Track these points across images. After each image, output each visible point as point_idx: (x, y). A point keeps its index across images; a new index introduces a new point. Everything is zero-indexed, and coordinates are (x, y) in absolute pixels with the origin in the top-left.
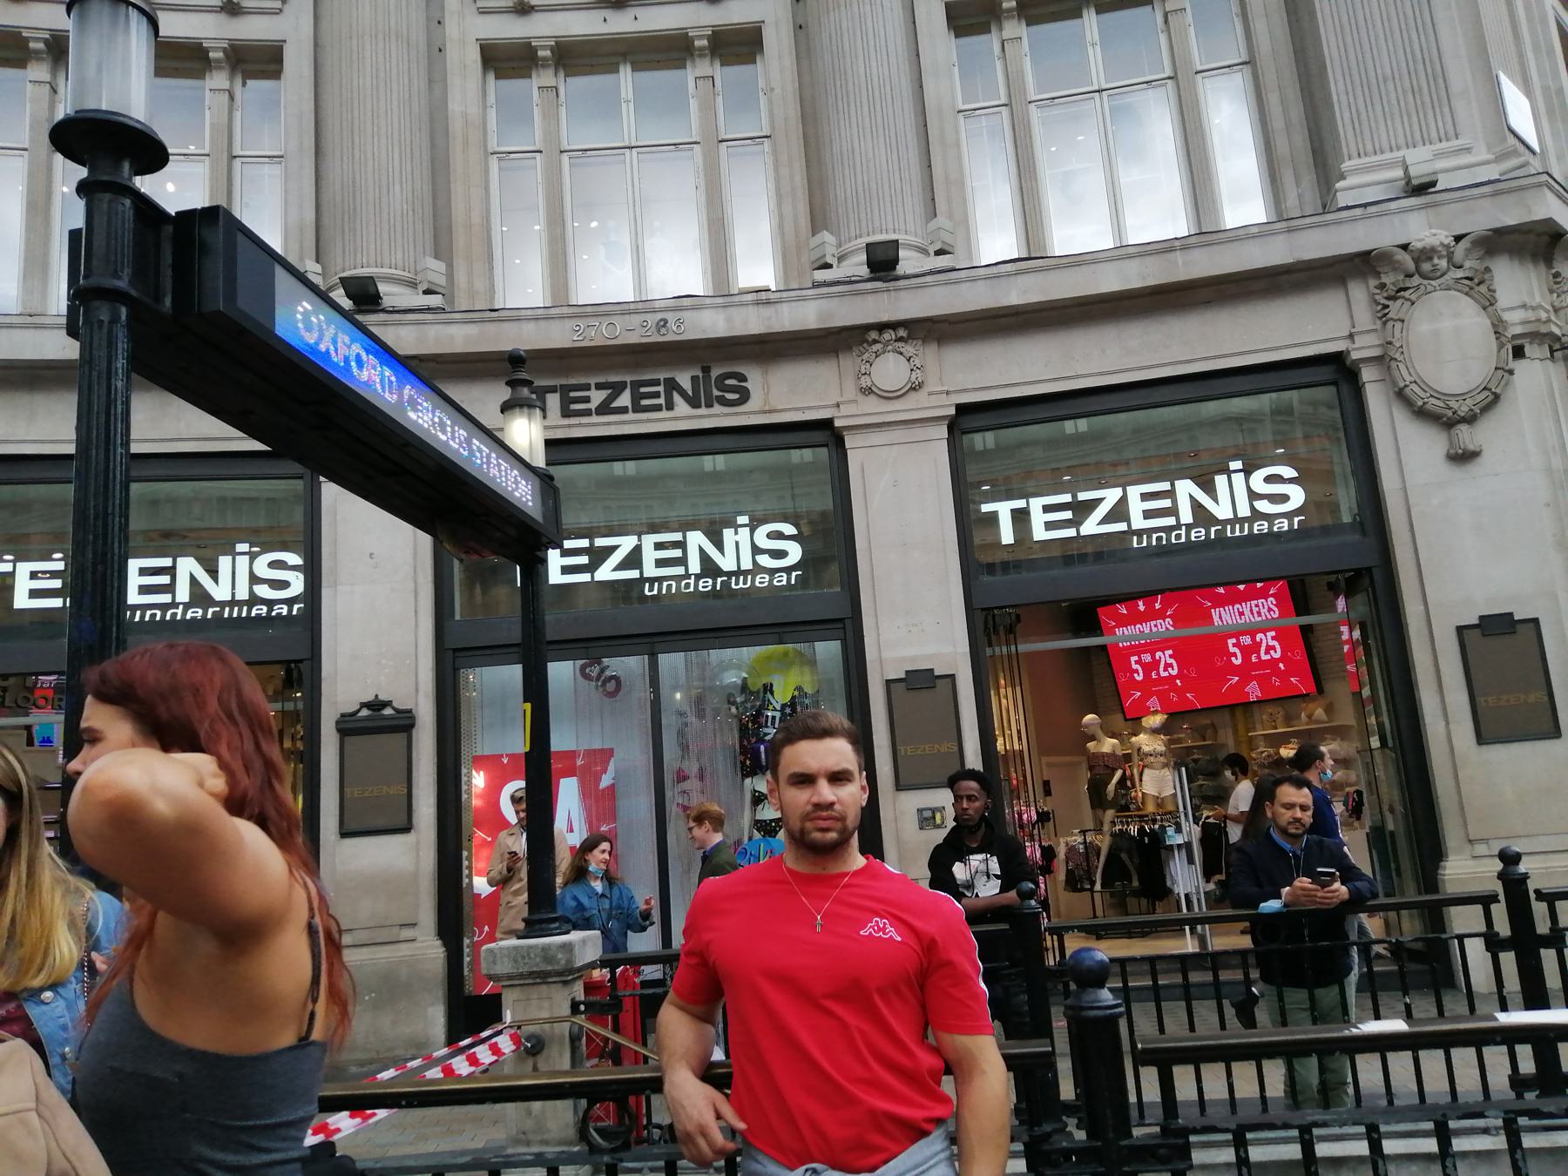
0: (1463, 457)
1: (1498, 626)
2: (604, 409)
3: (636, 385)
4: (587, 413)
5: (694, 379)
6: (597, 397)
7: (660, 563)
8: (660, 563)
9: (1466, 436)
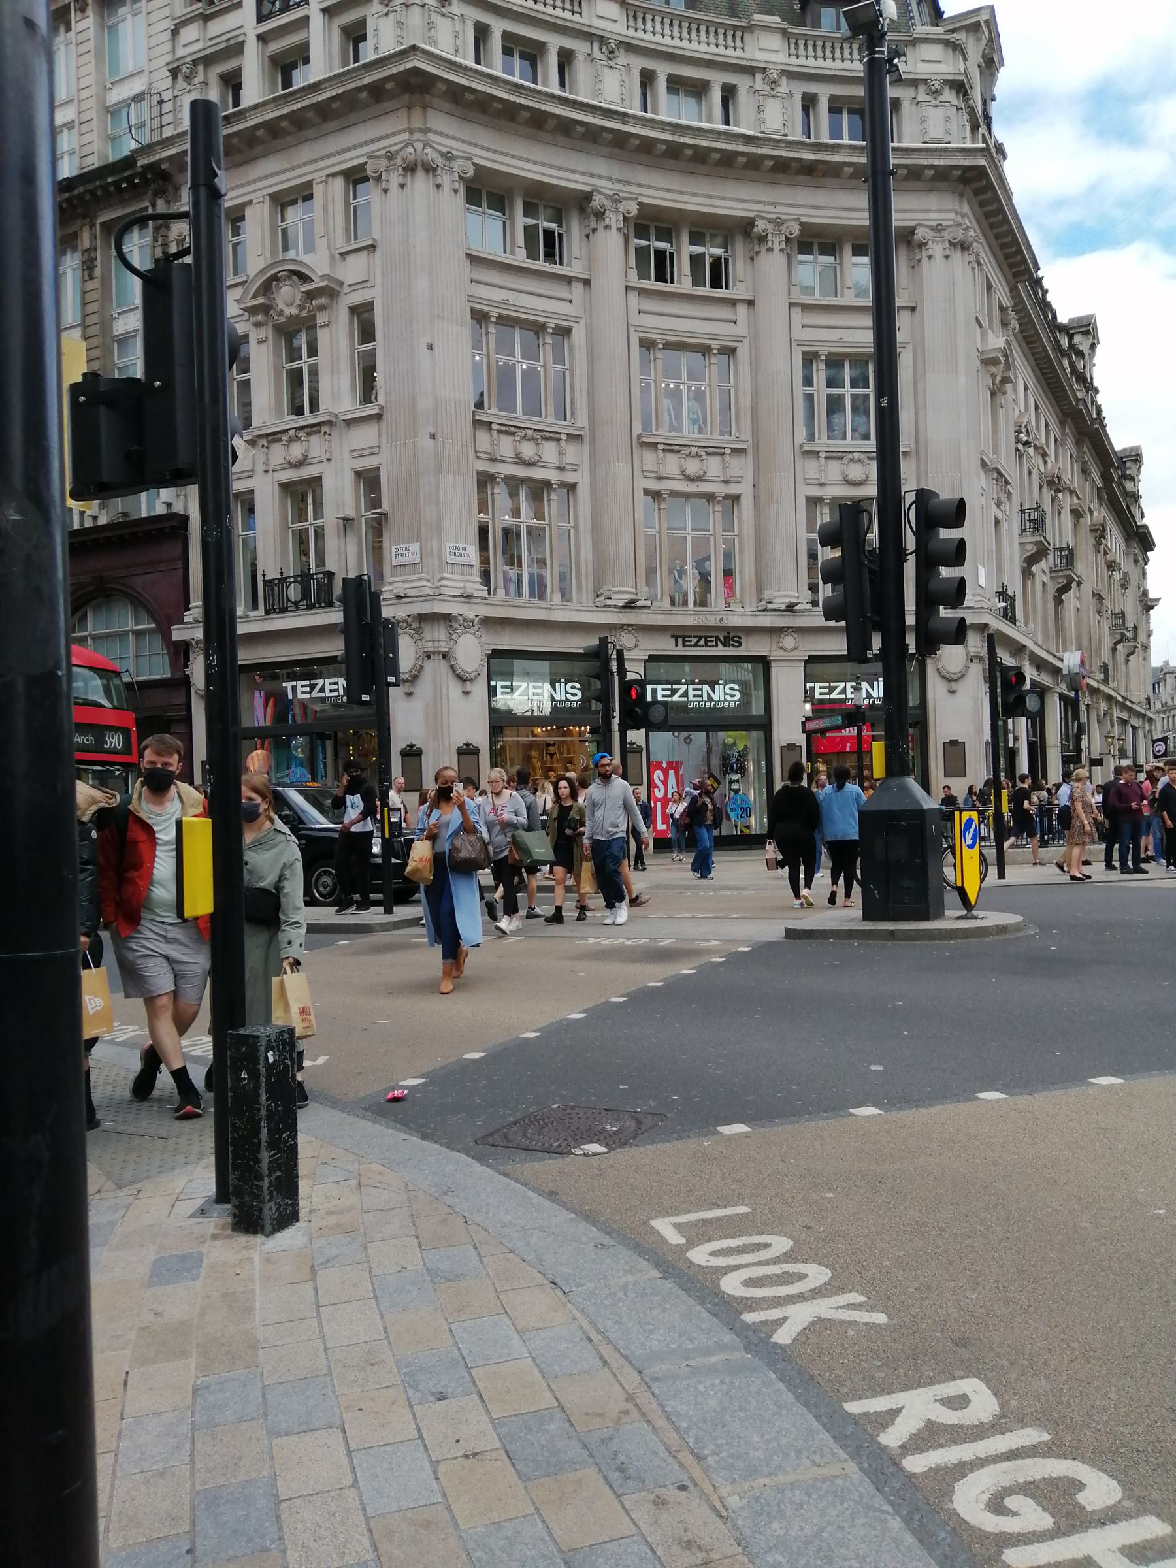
0: (952, 692)
1: (954, 743)
2: (696, 645)
3: (706, 637)
4: (690, 646)
5: (725, 637)
6: (694, 640)
7: (694, 696)
8: (694, 696)
9: (954, 686)
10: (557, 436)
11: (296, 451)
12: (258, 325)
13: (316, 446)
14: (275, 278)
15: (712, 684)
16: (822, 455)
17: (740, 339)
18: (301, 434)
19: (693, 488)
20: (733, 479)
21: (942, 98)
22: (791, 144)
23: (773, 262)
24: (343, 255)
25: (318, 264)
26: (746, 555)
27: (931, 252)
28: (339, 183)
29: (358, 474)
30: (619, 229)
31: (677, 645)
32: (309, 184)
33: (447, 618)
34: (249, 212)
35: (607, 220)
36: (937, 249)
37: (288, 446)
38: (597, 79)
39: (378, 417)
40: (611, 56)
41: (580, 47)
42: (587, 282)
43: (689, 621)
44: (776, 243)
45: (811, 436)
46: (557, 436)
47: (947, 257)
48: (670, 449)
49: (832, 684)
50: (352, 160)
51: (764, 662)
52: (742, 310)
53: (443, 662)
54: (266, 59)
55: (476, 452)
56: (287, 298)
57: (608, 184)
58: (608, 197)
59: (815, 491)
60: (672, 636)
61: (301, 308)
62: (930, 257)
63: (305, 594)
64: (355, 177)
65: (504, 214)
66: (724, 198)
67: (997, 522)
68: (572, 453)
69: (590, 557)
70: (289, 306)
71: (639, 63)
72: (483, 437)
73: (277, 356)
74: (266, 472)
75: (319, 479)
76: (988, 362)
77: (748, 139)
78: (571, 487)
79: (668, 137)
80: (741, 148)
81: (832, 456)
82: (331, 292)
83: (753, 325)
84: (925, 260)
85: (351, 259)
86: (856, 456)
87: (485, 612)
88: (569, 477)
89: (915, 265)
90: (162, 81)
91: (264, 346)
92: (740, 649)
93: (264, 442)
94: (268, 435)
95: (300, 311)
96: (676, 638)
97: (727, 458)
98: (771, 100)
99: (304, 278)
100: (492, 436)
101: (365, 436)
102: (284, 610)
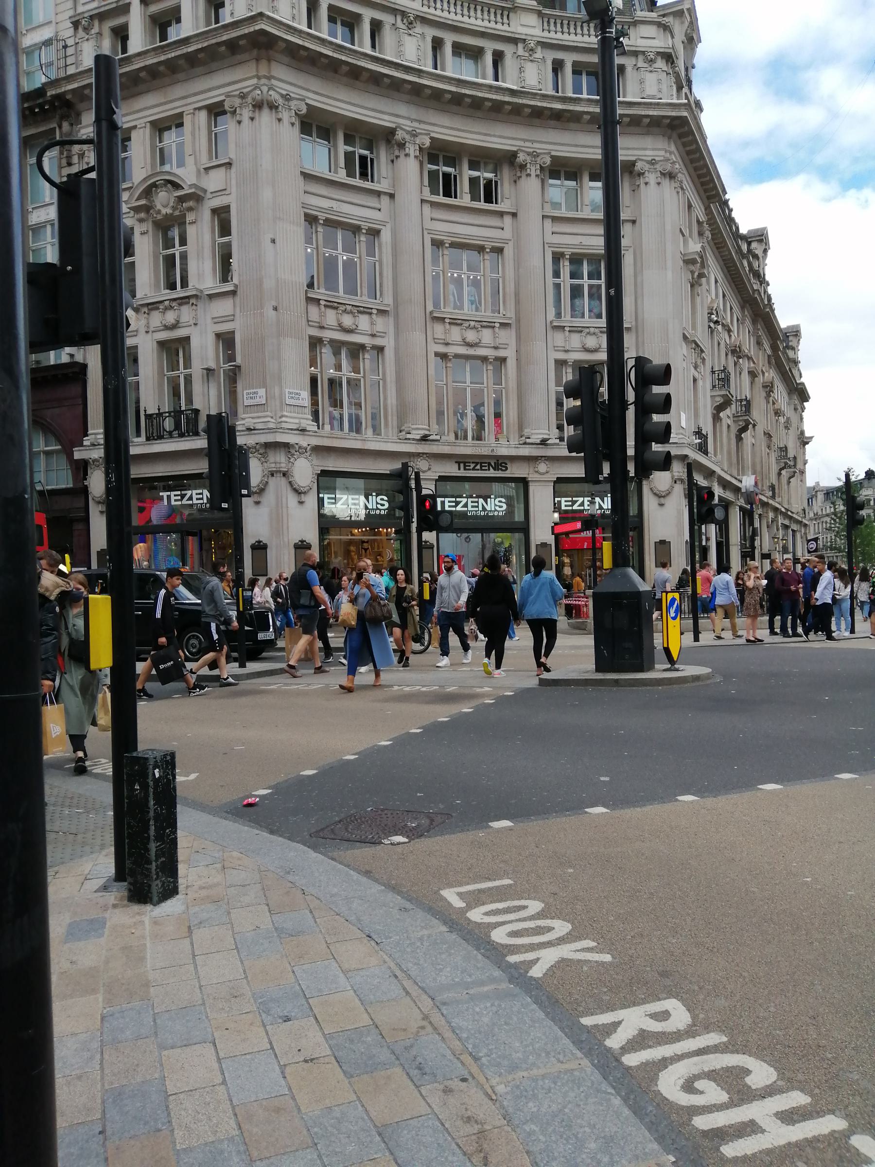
0: (661, 505)
1: (663, 542)
2: (474, 469)
3: (481, 463)
4: (470, 470)
5: (495, 463)
6: (472, 466)
7: (472, 507)
8: (472, 507)
9: (662, 500)
10: (370, 311)
11: (170, 317)
12: (141, 221)
13: (186, 313)
14: (154, 185)
15: (486, 498)
16: (567, 329)
17: (506, 241)
18: (174, 304)
19: (471, 352)
20: (501, 346)
21: (656, 65)
22: (545, 97)
23: (531, 185)
24: (207, 169)
25: (187, 175)
26: (511, 402)
27: (647, 180)
28: (203, 115)
29: (218, 336)
30: (416, 157)
31: (459, 469)
32: (180, 115)
33: (286, 446)
34: (134, 135)
35: (407, 149)
36: (652, 178)
37: (164, 313)
38: (400, 44)
39: (233, 293)
40: (410, 26)
41: (387, 19)
42: (392, 196)
43: (468, 451)
44: (533, 170)
45: (558, 315)
46: (370, 311)
47: (659, 184)
48: (454, 322)
49: (574, 499)
50: (214, 97)
51: (524, 483)
52: (508, 220)
53: (283, 479)
54: (147, 18)
55: (308, 321)
56: (164, 201)
57: (408, 123)
58: (408, 132)
59: (561, 356)
60: (456, 462)
61: (174, 208)
62: (646, 184)
63: (177, 426)
64: (216, 111)
65: (329, 143)
66: (494, 136)
67: (695, 380)
68: (380, 324)
69: (394, 402)
70: (165, 206)
71: (431, 32)
72: (314, 312)
73: (156, 244)
74: (147, 332)
75: (187, 339)
76: (689, 262)
77: (512, 92)
78: (380, 349)
79: (453, 89)
80: (507, 99)
81: (574, 330)
82: (197, 197)
83: (517, 232)
84: (642, 186)
85: (213, 173)
86: (592, 330)
87: (315, 442)
88: (378, 342)
89: (635, 189)
90: (67, 31)
91: (145, 237)
92: (506, 472)
93: (146, 309)
94: (148, 304)
95: (173, 211)
96: (459, 463)
97: (497, 330)
98: (530, 64)
99: (176, 186)
100: (320, 309)
101: (223, 307)
102: (161, 437)
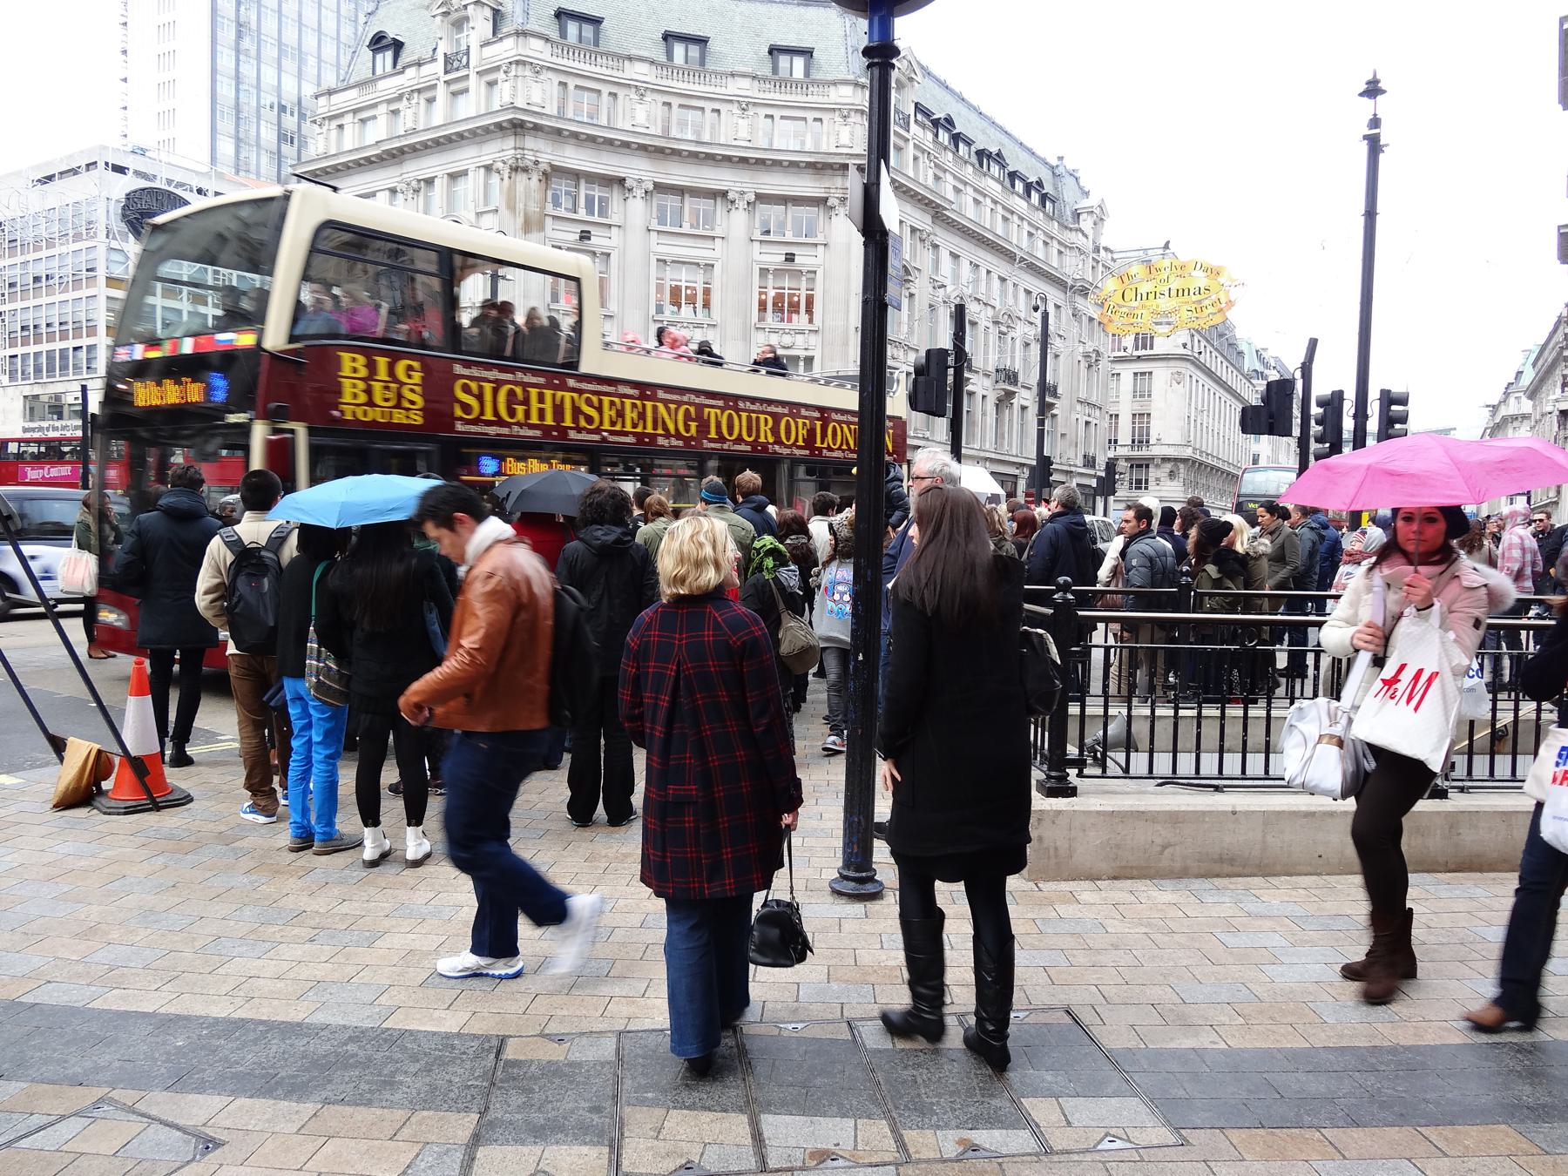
28: (482, 170)
32: (467, 170)
34: (436, 180)
45: (761, 319)
84: (834, 217)
85: (485, 217)
